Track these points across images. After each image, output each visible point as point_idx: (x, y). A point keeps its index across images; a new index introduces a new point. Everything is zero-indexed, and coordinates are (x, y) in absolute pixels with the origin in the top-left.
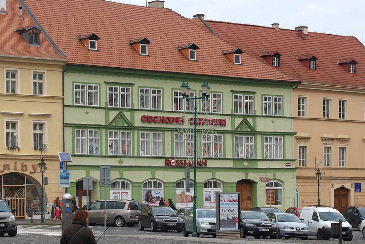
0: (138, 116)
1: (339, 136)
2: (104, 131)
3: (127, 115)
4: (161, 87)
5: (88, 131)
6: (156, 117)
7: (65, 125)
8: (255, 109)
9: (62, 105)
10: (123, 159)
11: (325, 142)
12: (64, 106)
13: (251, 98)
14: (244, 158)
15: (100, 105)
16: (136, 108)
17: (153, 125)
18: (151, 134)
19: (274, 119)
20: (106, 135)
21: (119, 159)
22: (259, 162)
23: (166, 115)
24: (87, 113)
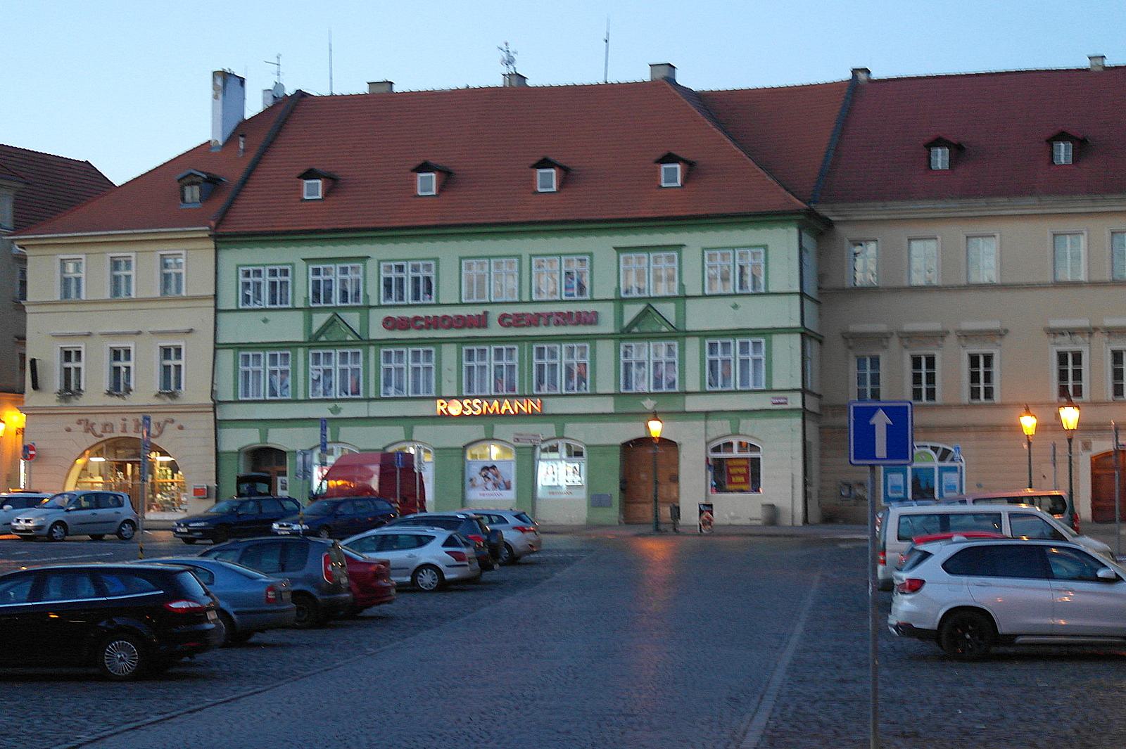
0: (377, 317)
1: (1109, 322)
2: (301, 351)
3: (353, 319)
4: (517, 253)
5: (268, 353)
6: (417, 318)
7: (217, 347)
8: (684, 282)
9: (213, 309)
10: (339, 405)
11: (1059, 339)
12: (217, 311)
13: (327, 272)
14: (647, 391)
15: (293, 303)
16: (373, 302)
17: (413, 334)
18: (408, 352)
19: (737, 300)
20: (306, 359)
21: (331, 405)
22: (688, 398)
23: (451, 312)
24: (735, 307)
